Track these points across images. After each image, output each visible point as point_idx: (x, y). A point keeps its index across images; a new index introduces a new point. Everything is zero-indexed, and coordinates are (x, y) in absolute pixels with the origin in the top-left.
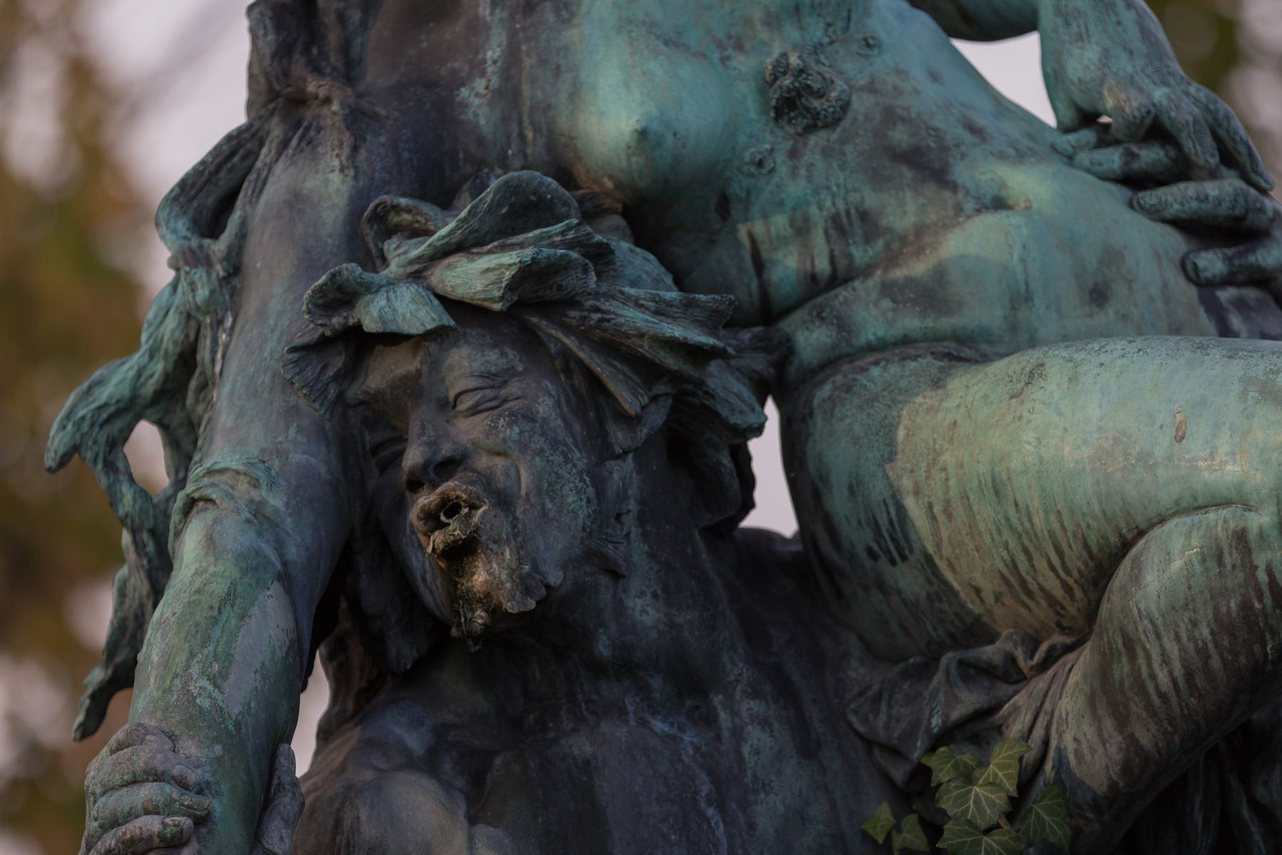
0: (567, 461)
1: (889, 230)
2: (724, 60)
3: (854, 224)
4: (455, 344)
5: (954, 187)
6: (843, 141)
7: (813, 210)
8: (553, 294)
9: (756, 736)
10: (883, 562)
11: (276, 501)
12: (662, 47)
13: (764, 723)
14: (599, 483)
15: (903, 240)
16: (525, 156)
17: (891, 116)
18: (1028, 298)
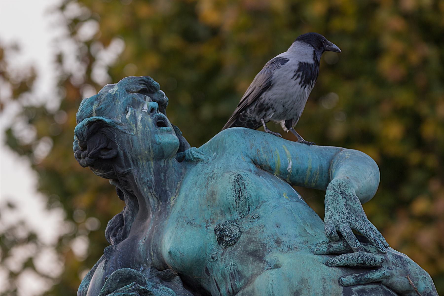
1: (245, 276)
2: (206, 227)
3: (237, 275)
6: (235, 250)
12: (185, 225)
15: (248, 279)
16: (152, 260)
17: (250, 241)
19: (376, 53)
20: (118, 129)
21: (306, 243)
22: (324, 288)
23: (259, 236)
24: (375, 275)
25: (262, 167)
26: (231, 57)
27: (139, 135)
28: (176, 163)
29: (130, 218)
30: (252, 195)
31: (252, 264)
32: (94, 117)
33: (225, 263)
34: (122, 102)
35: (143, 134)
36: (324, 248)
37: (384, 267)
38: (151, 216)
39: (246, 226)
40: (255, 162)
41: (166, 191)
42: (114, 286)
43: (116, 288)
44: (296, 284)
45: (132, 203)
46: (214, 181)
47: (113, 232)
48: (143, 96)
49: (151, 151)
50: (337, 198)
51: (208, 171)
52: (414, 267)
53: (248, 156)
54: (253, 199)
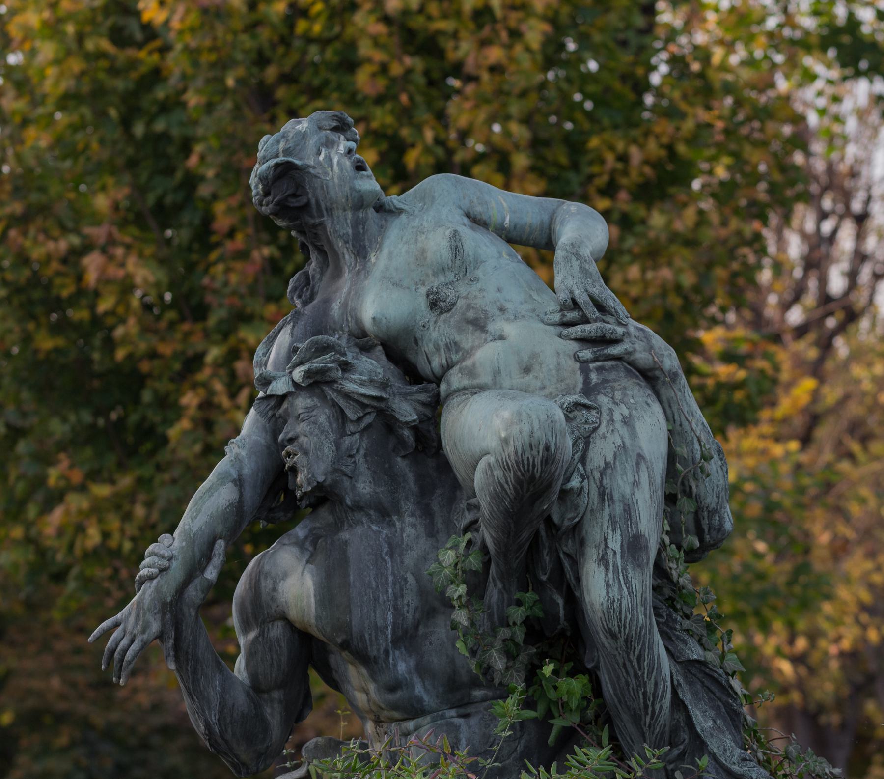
0: (326, 437)
3: (453, 346)
4: (297, 397)
5: (486, 332)
6: (451, 317)
7: (440, 343)
8: (328, 379)
9: (409, 530)
11: (243, 453)
12: (391, 287)
13: (414, 525)
14: (338, 445)
15: (467, 352)
17: (469, 307)
18: (499, 372)
19: (349, 64)
20: (309, 173)
21: (534, 310)
22: (559, 364)
23: (479, 302)
24: (616, 350)
25: (477, 221)
26: (176, 64)
27: (336, 180)
28: (375, 213)
29: (318, 276)
30: (470, 254)
31: (472, 334)
32: (281, 159)
33: (438, 331)
34: (315, 140)
35: (340, 178)
36: (557, 317)
37: (626, 340)
38: (346, 275)
39: (463, 290)
40: (468, 215)
41: (365, 246)
42: (308, 356)
43: (310, 359)
44: (526, 358)
45: (320, 259)
46: (424, 237)
47: (297, 293)
48: (337, 135)
49: (350, 199)
50: (571, 259)
51: (416, 224)
52: (658, 341)
53: (460, 208)
54: (471, 259)
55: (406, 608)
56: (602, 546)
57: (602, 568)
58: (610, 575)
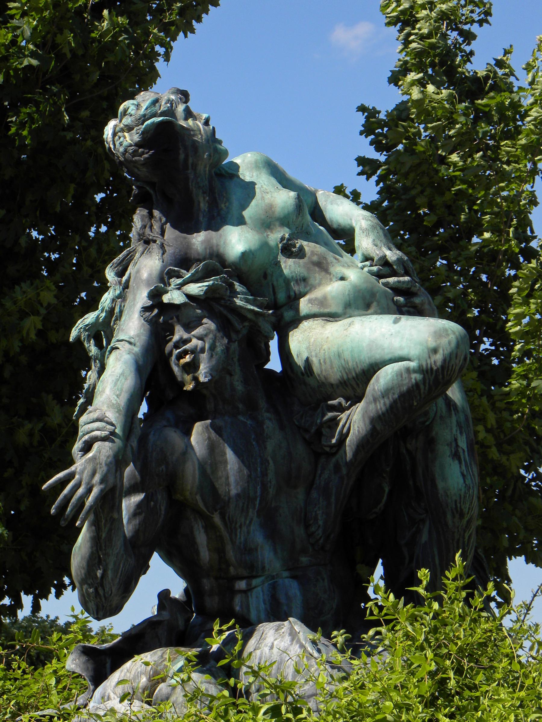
5: (330, 274)
8: (217, 296)
10: (306, 376)
13: (270, 419)
55: (269, 484)
56: (454, 444)
57: (457, 462)
58: (464, 467)
